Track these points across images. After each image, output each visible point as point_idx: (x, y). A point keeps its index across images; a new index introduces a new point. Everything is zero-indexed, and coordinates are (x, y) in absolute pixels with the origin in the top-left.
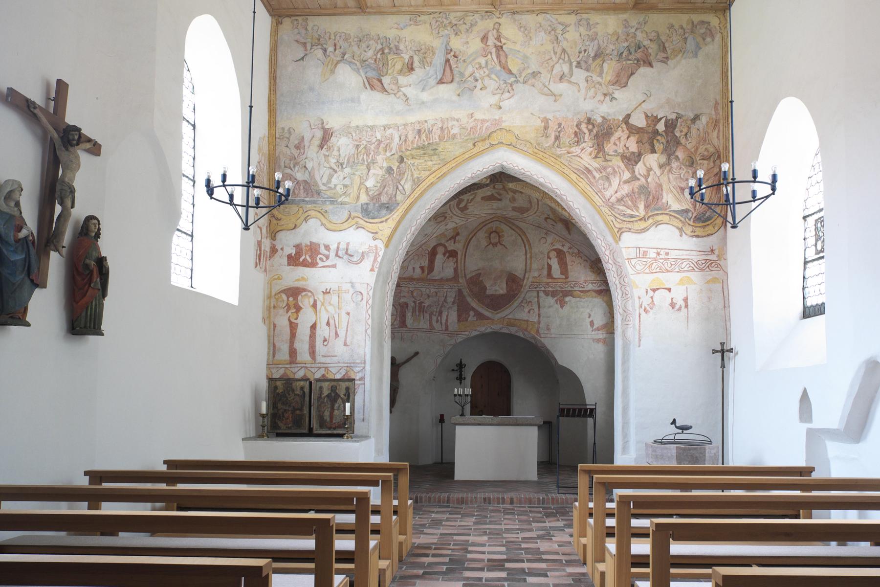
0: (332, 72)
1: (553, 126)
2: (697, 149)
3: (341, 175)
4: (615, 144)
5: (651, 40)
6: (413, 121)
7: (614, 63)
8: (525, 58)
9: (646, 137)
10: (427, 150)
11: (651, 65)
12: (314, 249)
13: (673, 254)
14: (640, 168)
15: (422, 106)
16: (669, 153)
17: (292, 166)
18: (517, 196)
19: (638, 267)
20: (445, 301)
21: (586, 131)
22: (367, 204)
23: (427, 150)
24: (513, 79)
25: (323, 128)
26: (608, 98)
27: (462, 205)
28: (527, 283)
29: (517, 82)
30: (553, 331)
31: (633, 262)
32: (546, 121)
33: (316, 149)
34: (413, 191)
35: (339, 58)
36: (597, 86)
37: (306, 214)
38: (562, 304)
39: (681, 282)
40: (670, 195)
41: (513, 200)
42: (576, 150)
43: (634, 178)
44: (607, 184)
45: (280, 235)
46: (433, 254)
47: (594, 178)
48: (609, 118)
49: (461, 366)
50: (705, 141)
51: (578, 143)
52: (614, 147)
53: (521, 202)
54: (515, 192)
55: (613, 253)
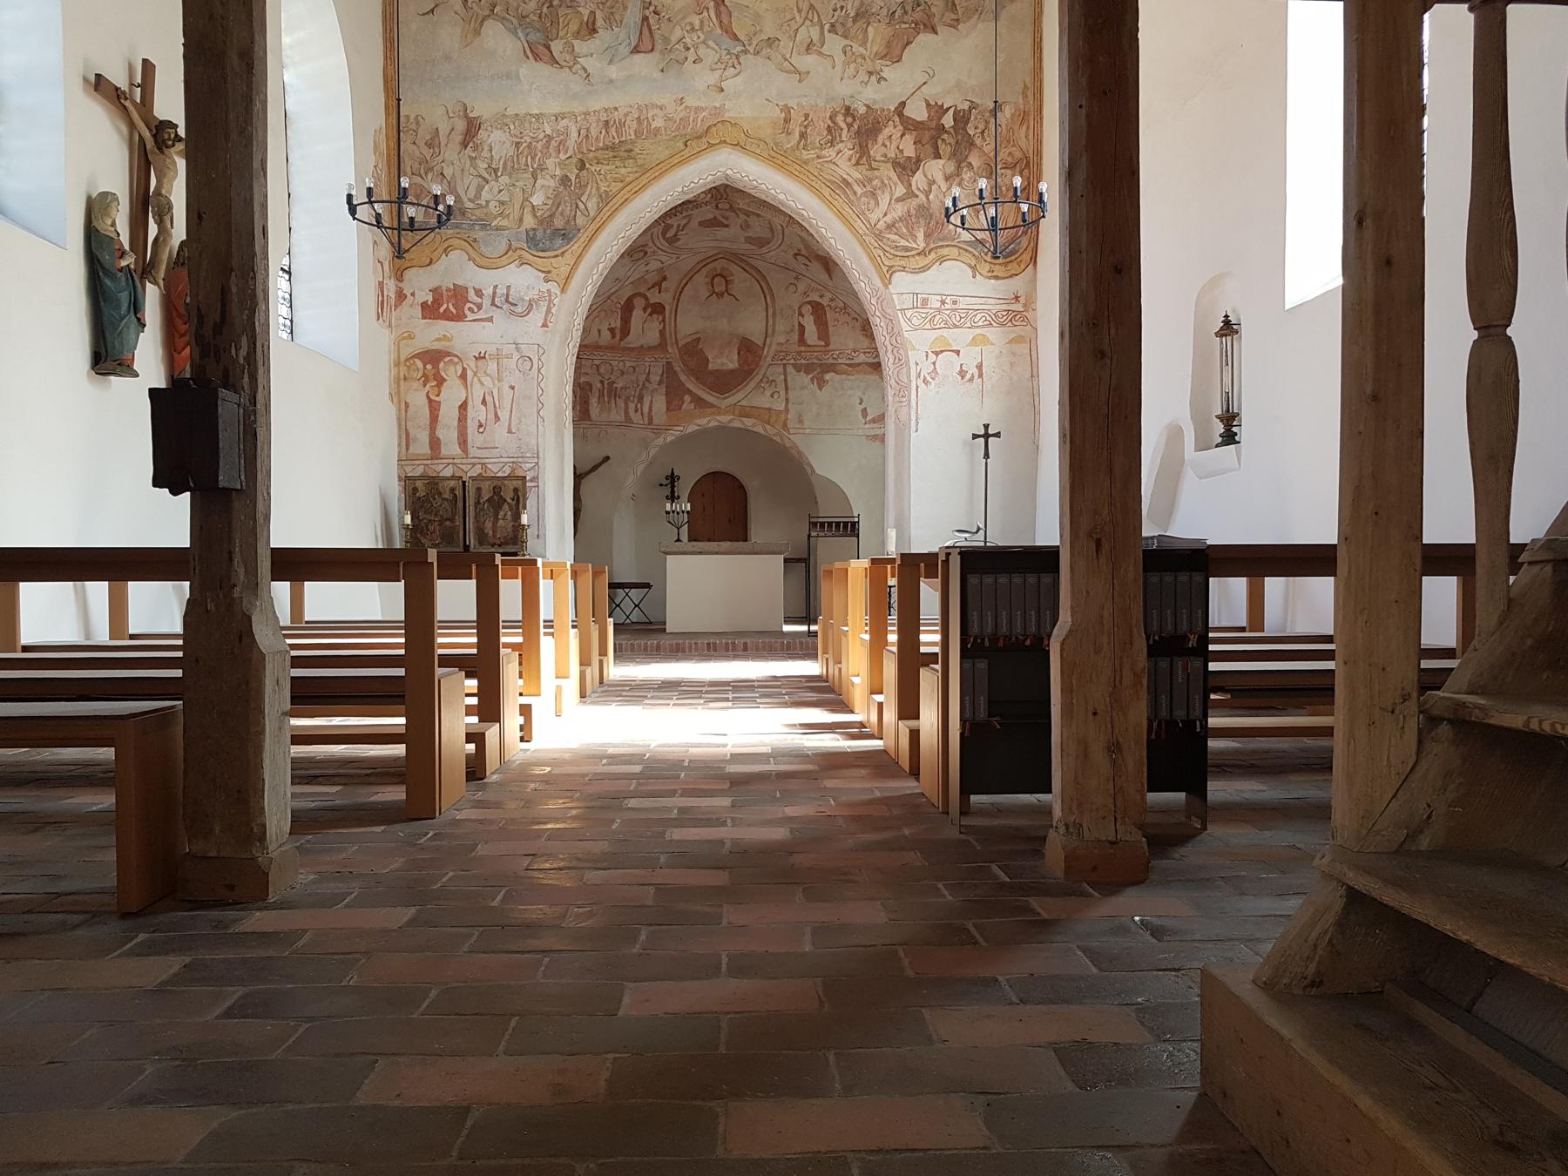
0: (477, 32)
1: (798, 119)
3: (495, 186)
4: (884, 145)
7: (882, 27)
8: (757, 15)
9: (927, 136)
10: (619, 151)
12: (459, 294)
14: (918, 180)
15: (611, 83)
16: (959, 158)
18: (752, 220)
20: (647, 379)
21: (843, 126)
23: (619, 151)
24: (739, 48)
25: (466, 116)
26: (874, 78)
27: (670, 234)
28: (768, 353)
29: (745, 52)
30: (807, 423)
32: (787, 110)
33: (458, 148)
34: (600, 210)
35: (487, 12)
38: (821, 383)
41: (746, 226)
42: (830, 153)
43: (910, 194)
45: (409, 274)
46: (628, 308)
49: (672, 479)
51: (832, 143)
53: (758, 230)
54: (747, 214)
55: (880, 300)
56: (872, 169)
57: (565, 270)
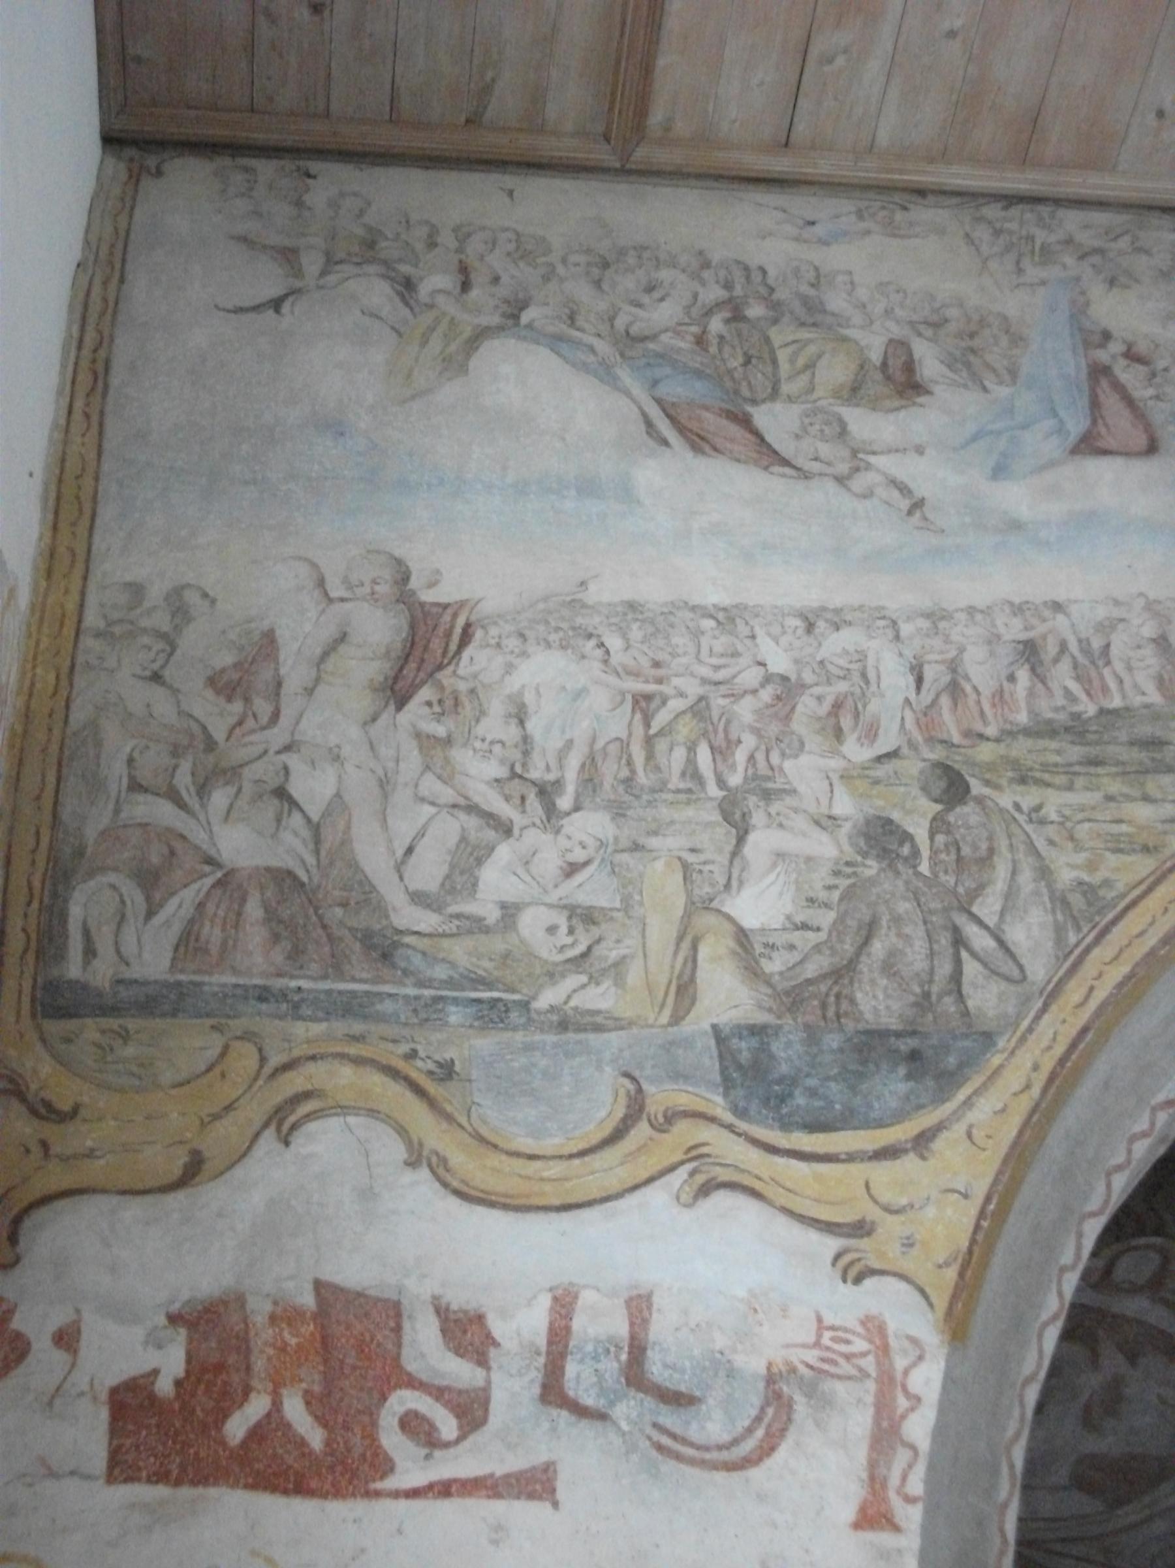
0: (456, 364)
6: (980, 601)
12: (350, 1342)
17: (183, 780)
22: (756, 1030)
33: (363, 703)
34: (1072, 963)
37: (295, 1082)
57: (949, 1224)
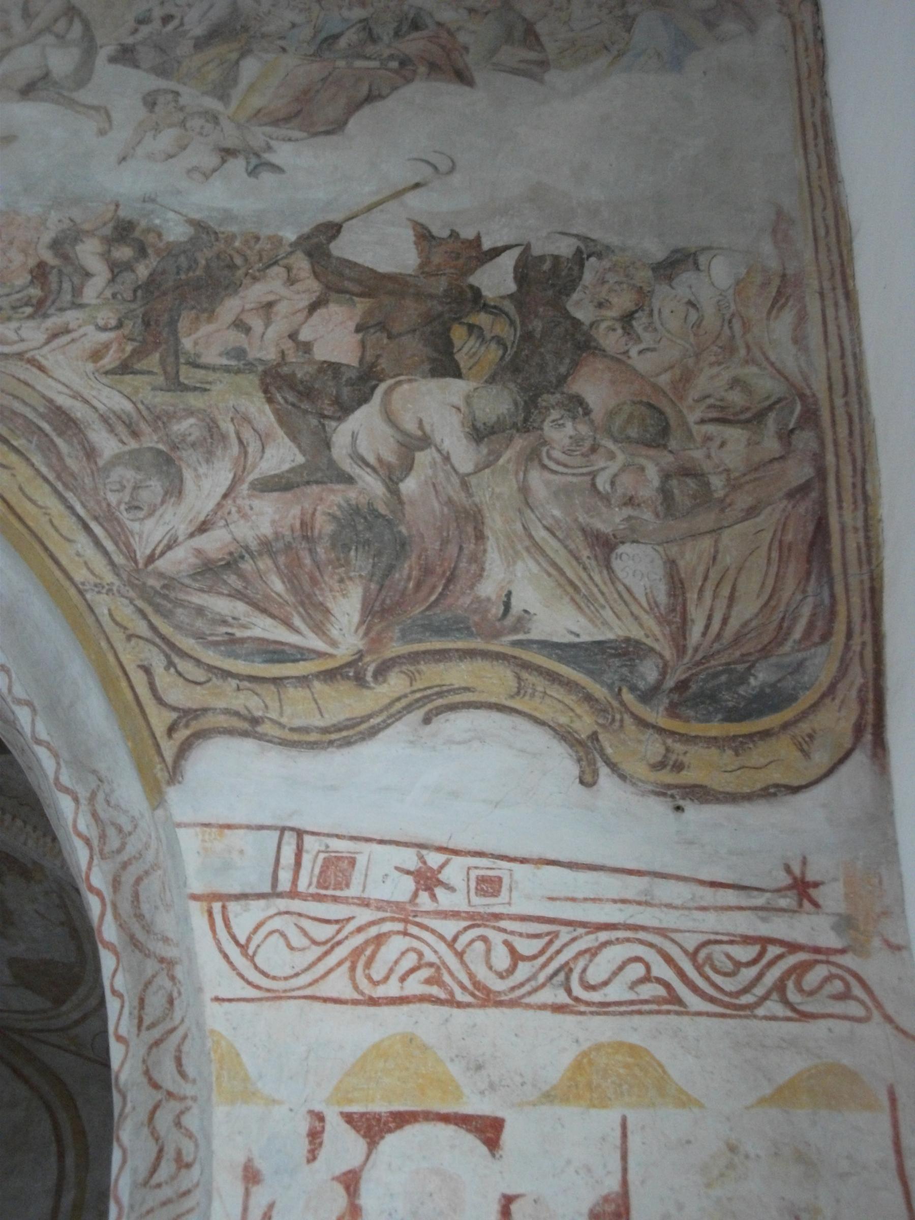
2: (686, 378)
4: (240, 325)
5: (471, 11)
11: (462, 77)
13: (527, 892)
14: (362, 432)
19: (274, 957)
26: (237, 165)
31: (244, 918)
36: (196, 123)
39: (582, 1083)
40: (527, 567)
43: (321, 470)
44: (156, 486)
47: (90, 453)
48: (234, 229)
50: (730, 349)
51: (39, 309)
52: (235, 338)
56: (176, 385)
